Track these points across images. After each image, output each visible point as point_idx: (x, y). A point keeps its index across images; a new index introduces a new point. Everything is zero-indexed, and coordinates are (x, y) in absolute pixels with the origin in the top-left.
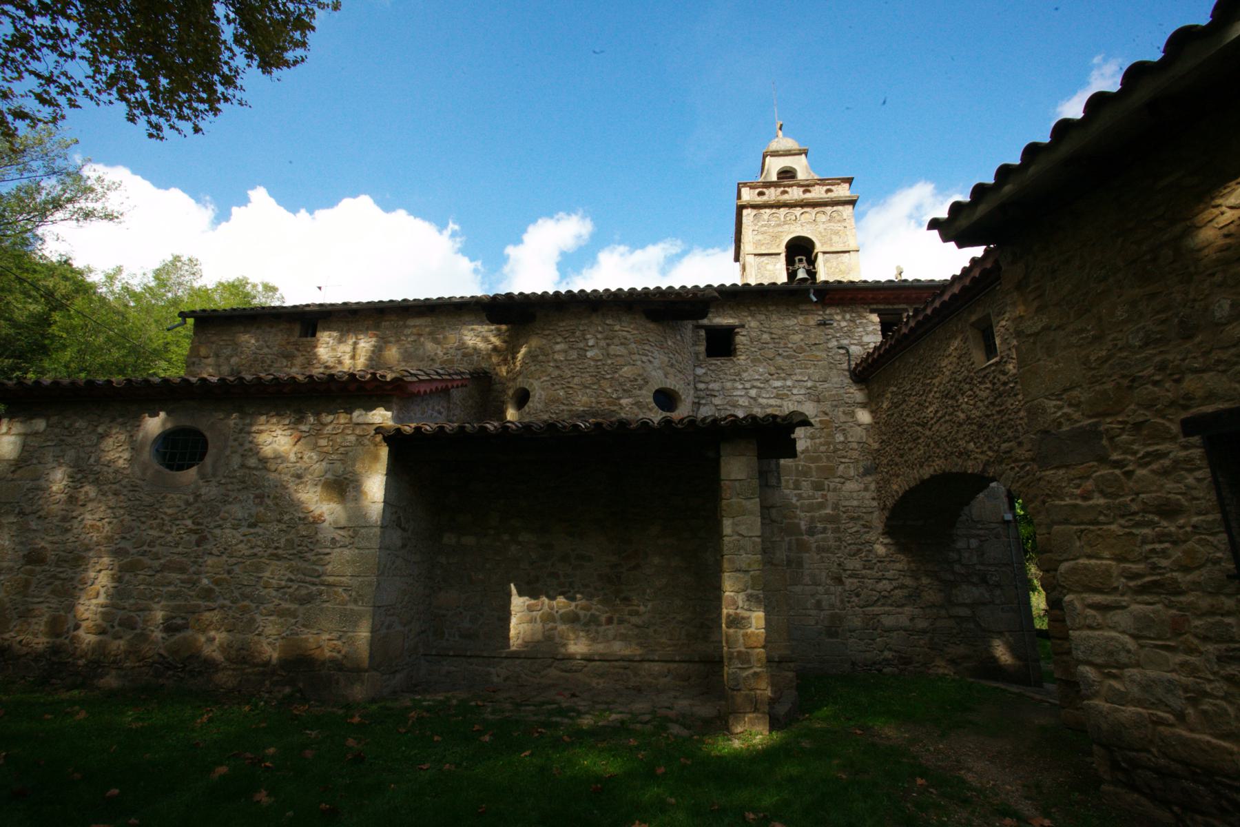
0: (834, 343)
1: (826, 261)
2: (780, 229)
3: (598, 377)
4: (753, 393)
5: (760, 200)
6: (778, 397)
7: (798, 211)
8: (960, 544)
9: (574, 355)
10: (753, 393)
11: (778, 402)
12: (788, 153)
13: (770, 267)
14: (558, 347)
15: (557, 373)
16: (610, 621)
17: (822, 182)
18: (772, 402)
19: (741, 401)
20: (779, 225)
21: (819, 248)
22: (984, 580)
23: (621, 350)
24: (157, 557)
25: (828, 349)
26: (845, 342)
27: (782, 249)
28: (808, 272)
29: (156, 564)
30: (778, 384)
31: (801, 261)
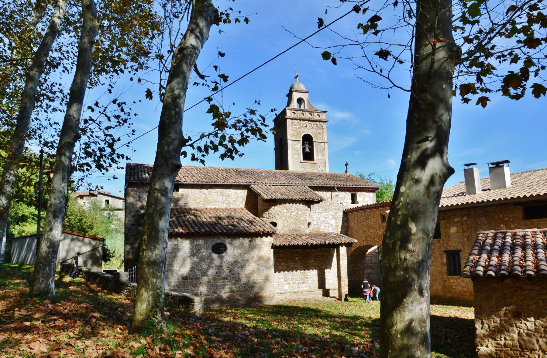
0: (339, 202)
1: (316, 145)
2: (300, 130)
3: (296, 220)
4: (319, 216)
5: (294, 116)
6: (325, 218)
7: (307, 123)
8: (367, 259)
9: (289, 214)
10: (319, 216)
11: (325, 219)
12: (302, 92)
13: (296, 146)
14: (285, 211)
15: (285, 219)
16: (303, 283)
17: (317, 111)
18: (324, 219)
19: (316, 219)
20: (300, 128)
21: (314, 140)
22: (371, 268)
23: (300, 212)
24: (219, 276)
25: (338, 204)
26: (342, 202)
27: (301, 140)
28: (309, 149)
29: (219, 278)
30: (325, 214)
31: (307, 143)
